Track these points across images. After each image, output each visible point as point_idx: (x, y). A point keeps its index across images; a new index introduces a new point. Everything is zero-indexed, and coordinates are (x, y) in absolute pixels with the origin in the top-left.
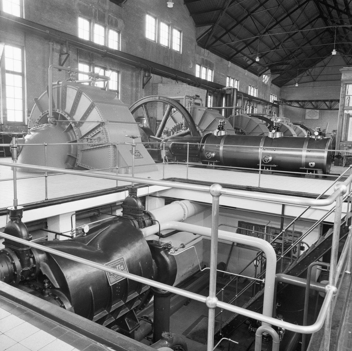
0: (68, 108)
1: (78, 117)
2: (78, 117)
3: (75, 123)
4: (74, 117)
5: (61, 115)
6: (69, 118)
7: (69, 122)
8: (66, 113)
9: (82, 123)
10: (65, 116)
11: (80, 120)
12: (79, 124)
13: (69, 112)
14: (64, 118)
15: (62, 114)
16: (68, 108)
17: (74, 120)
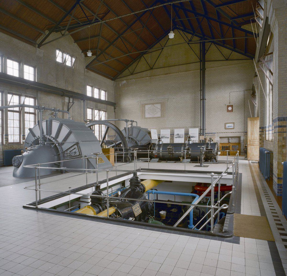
0: (54, 134)
1: (60, 139)
2: (60, 139)
3: (59, 143)
4: (58, 140)
5: (48, 138)
6: (54, 140)
7: (54, 143)
8: (52, 137)
9: (64, 143)
10: (51, 139)
13: (54, 136)
14: (51, 141)
15: (49, 138)
16: (54, 134)
17: (58, 141)
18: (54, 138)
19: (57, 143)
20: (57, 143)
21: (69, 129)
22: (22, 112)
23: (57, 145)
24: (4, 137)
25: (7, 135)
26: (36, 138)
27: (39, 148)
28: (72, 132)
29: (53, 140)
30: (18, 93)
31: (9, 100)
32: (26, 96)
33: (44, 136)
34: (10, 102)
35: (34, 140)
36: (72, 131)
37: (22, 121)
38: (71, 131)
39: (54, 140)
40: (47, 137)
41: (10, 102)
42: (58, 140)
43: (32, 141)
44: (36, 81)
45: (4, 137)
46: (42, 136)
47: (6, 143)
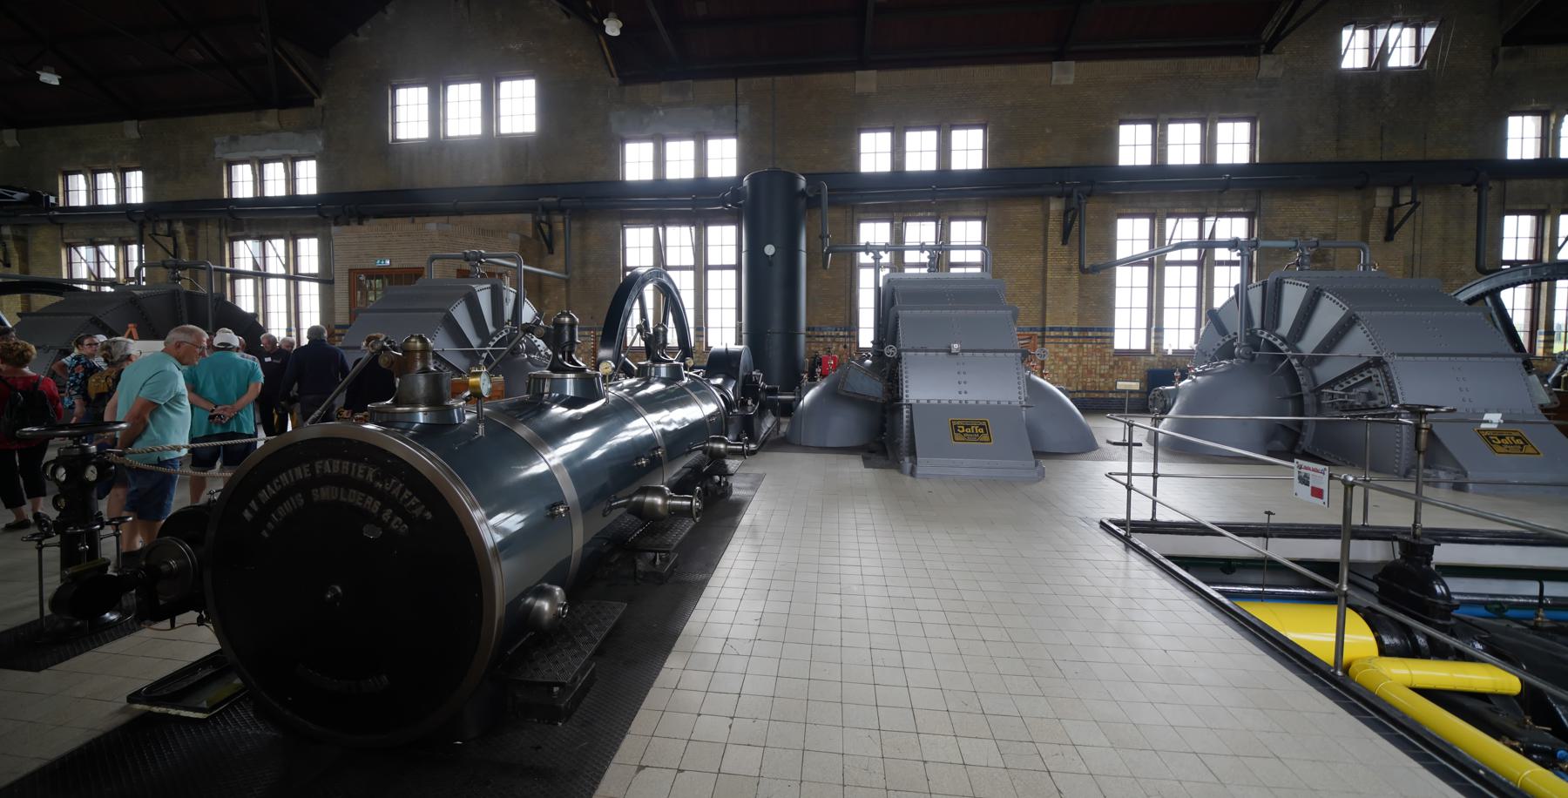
0: (1285, 328)
1: (1308, 344)
2: (1308, 344)
3: (1301, 359)
4: (1301, 345)
6: (1284, 347)
7: (1285, 356)
10: (1275, 342)
11: (1315, 351)
12: (1315, 360)
14: (1275, 348)
15: (1270, 339)
16: (1285, 328)
17: (1300, 351)
18: (1284, 340)
19: (1293, 357)
20: (1293, 357)
21: (1347, 308)
22: (1205, 263)
23: (1294, 362)
24: (1153, 334)
25: (1160, 330)
26: (1227, 339)
27: (1232, 369)
28: (1358, 318)
29: (1281, 348)
30: (1195, 210)
31: (1168, 236)
32: (1220, 215)
33: (1253, 333)
34: (1171, 239)
35: (1222, 343)
36: (1357, 313)
37: (1205, 287)
38: (1354, 315)
39: (1284, 347)
40: (1263, 336)
41: (1171, 239)
42: (1301, 345)
43: (1217, 348)
44: (1257, 161)
45: (1153, 334)
46: (1246, 331)
47: (1157, 350)
